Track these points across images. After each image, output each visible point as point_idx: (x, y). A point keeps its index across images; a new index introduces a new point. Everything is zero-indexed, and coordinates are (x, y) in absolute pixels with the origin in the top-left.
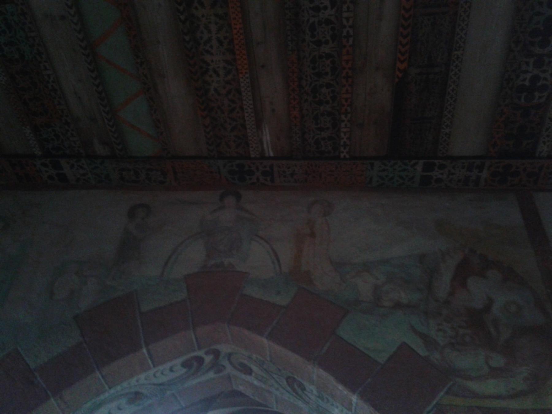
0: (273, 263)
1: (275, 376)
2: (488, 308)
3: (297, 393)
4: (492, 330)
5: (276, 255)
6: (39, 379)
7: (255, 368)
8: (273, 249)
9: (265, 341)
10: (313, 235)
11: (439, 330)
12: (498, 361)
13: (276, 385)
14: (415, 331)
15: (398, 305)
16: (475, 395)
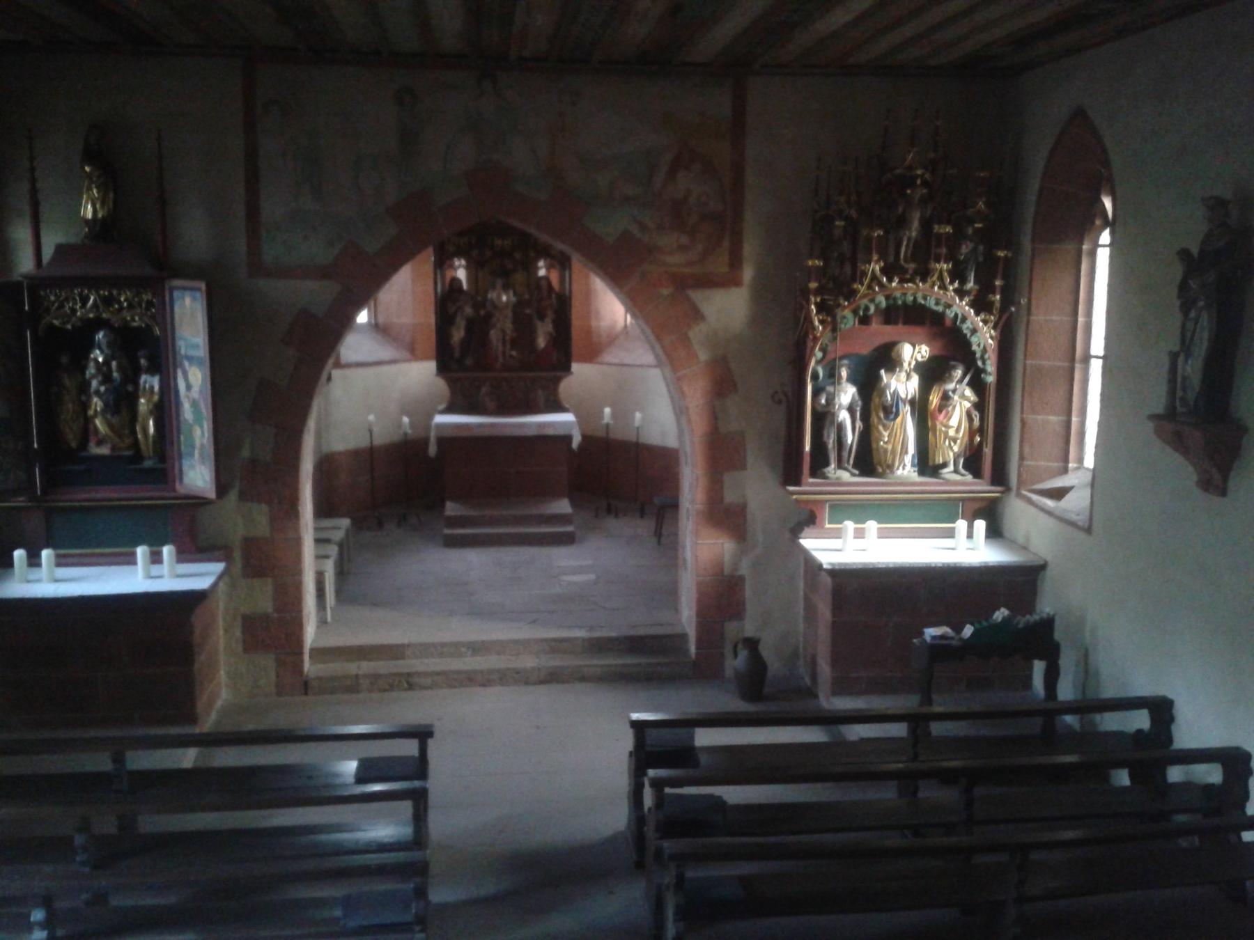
12: (684, 240)
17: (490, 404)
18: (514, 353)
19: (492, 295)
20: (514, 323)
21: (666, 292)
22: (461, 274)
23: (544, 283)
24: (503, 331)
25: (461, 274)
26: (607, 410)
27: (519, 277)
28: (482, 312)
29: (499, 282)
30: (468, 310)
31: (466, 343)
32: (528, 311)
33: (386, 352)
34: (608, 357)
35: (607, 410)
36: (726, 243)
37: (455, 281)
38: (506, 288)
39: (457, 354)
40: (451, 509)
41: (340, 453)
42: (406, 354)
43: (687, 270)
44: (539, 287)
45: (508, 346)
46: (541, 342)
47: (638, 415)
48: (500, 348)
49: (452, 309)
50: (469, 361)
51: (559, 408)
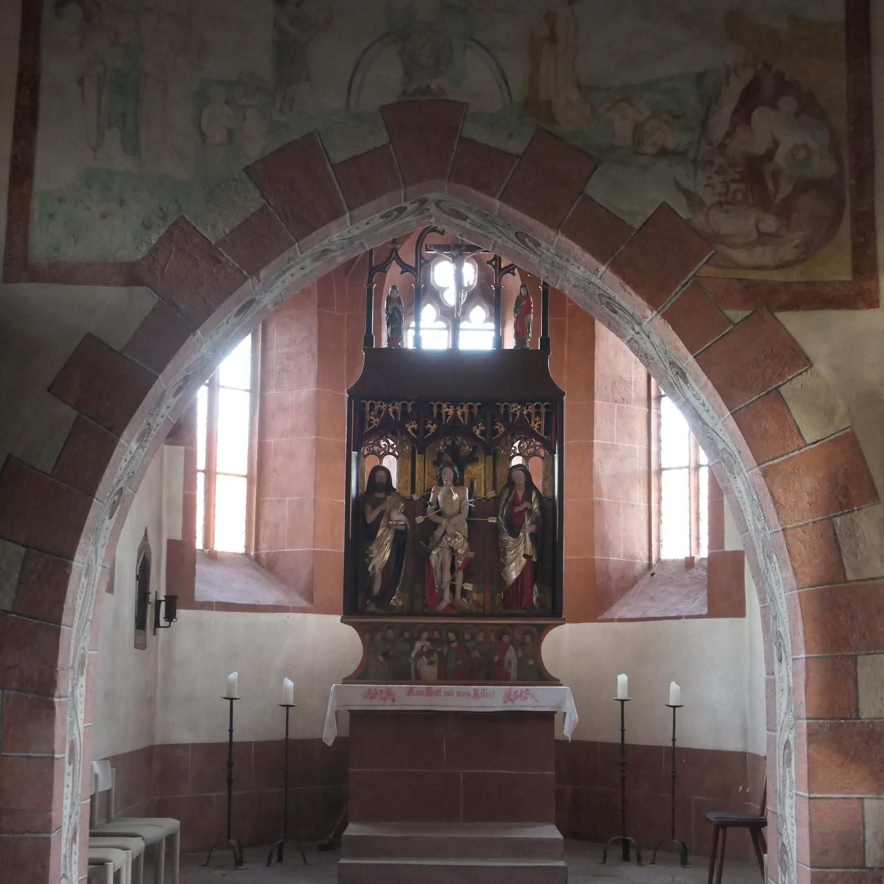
0: (500, 87)
1: (500, 228)
2: (770, 155)
3: (528, 247)
4: (770, 184)
5: (503, 75)
6: (225, 254)
7: (470, 215)
8: (498, 64)
9: (497, 203)
10: (553, 39)
11: (707, 185)
12: (770, 224)
13: (499, 234)
14: (678, 187)
15: (663, 152)
16: (738, 266)
17: (429, 670)
18: (469, 587)
19: (438, 495)
20: (470, 539)
21: (736, 315)
22: (390, 463)
23: (520, 476)
24: (453, 551)
25: (390, 463)
26: (622, 678)
27: (478, 470)
28: (420, 519)
29: (448, 474)
30: (398, 517)
31: (392, 570)
32: (492, 520)
33: (270, 595)
34: (620, 610)
35: (622, 678)
36: (845, 232)
37: (380, 471)
38: (458, 483)
39: (377, 588)
40: (353, 830)
41: (185, 747)
42: (302, 602)
43: (778, 277)
44: (511, 484)
45: (460, 575)
46: (513, 574)
47: (674, 686)
48: (447, 577)
49: (371, 518)
50: (396, 601)
51: (543, 678)
